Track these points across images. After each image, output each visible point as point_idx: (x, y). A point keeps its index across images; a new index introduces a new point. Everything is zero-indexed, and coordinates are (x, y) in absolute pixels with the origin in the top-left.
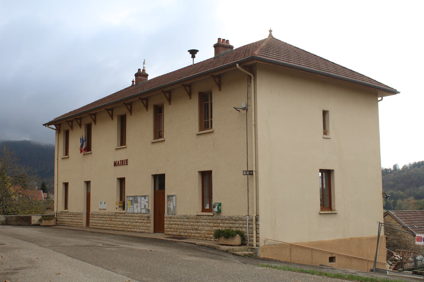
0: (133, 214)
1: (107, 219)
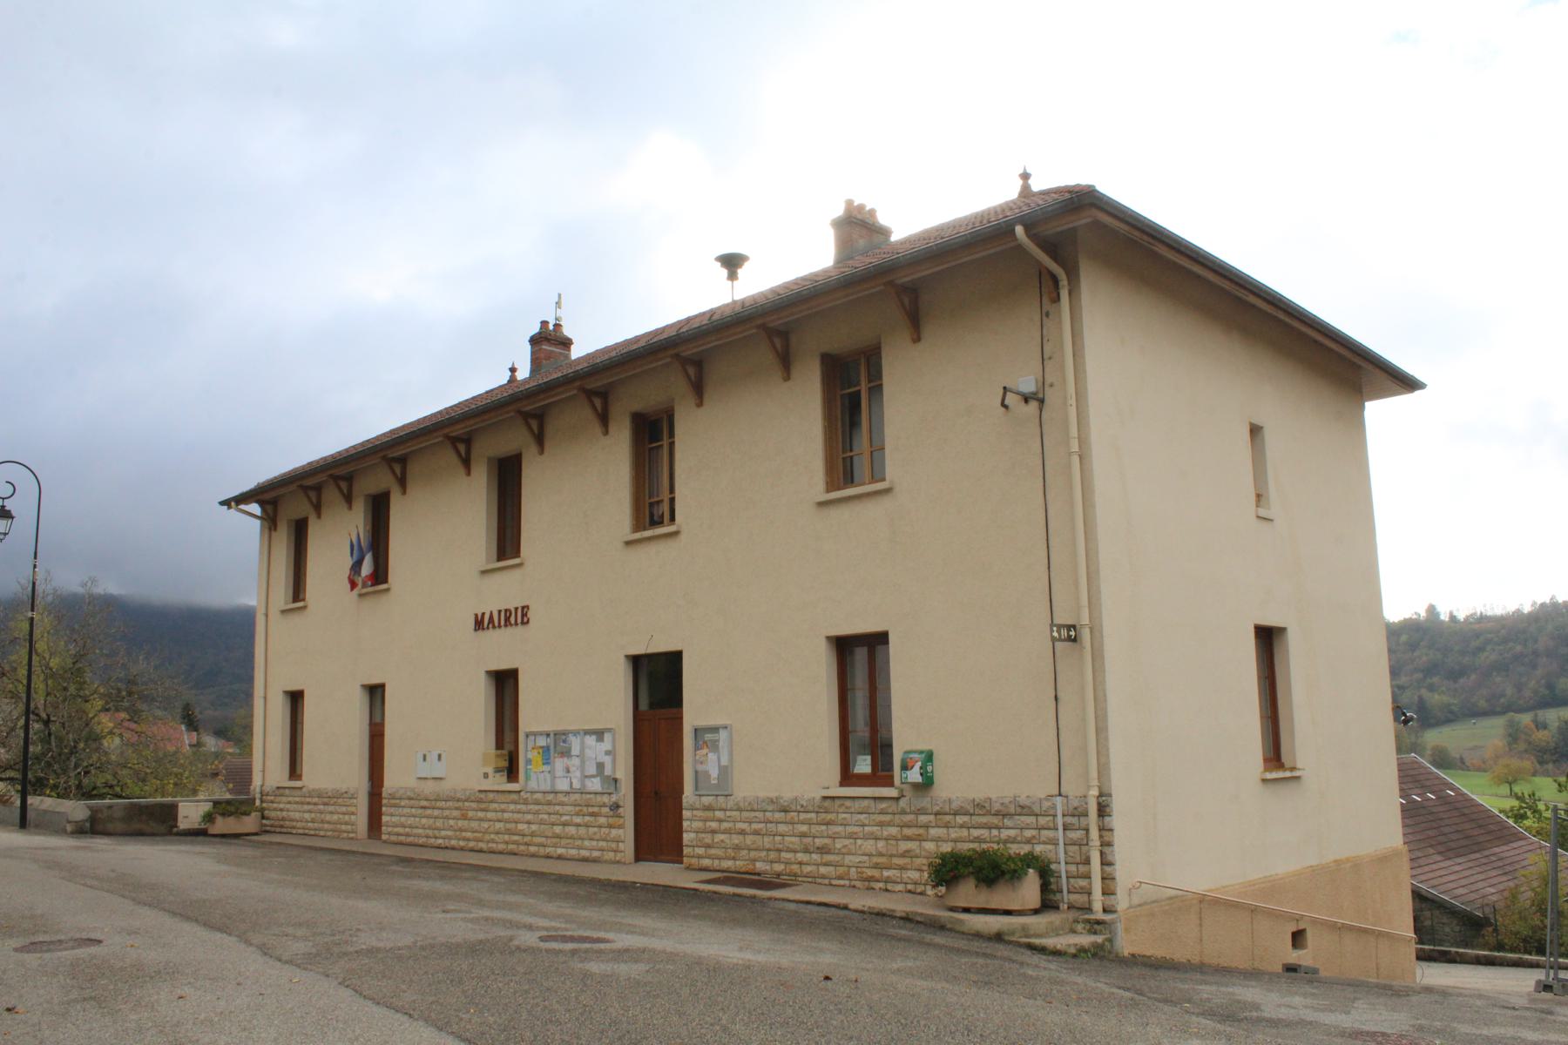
0: (550, 797)
1: (447, 813)
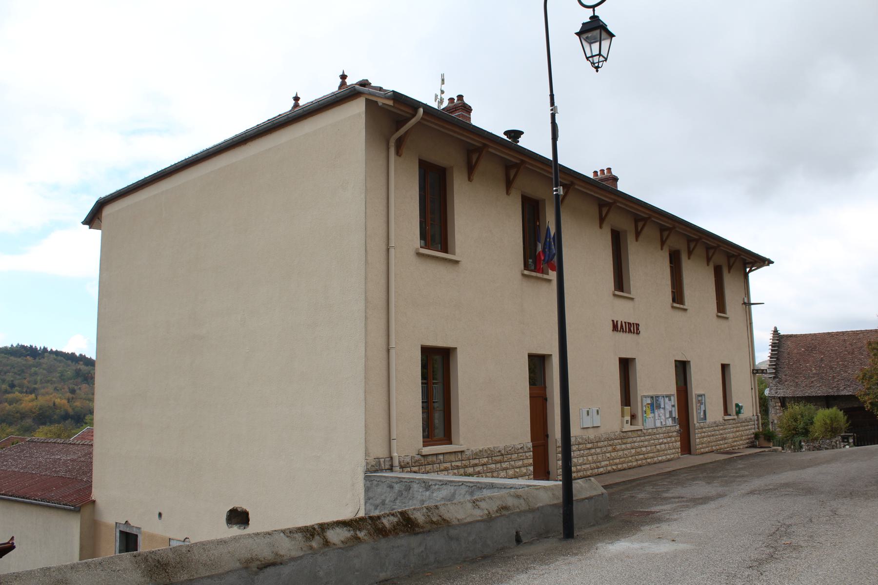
0: (655, 431)
1: (604, 449)
